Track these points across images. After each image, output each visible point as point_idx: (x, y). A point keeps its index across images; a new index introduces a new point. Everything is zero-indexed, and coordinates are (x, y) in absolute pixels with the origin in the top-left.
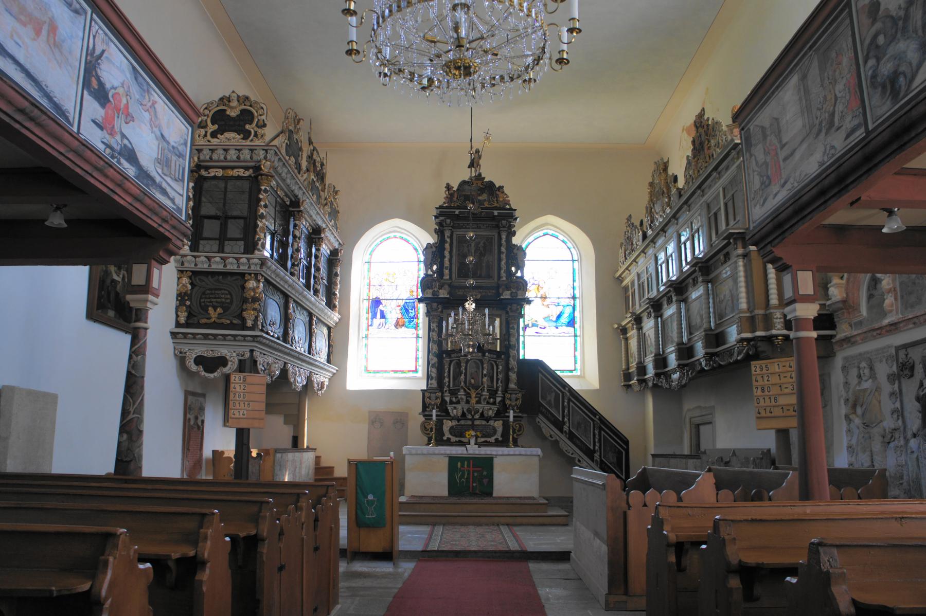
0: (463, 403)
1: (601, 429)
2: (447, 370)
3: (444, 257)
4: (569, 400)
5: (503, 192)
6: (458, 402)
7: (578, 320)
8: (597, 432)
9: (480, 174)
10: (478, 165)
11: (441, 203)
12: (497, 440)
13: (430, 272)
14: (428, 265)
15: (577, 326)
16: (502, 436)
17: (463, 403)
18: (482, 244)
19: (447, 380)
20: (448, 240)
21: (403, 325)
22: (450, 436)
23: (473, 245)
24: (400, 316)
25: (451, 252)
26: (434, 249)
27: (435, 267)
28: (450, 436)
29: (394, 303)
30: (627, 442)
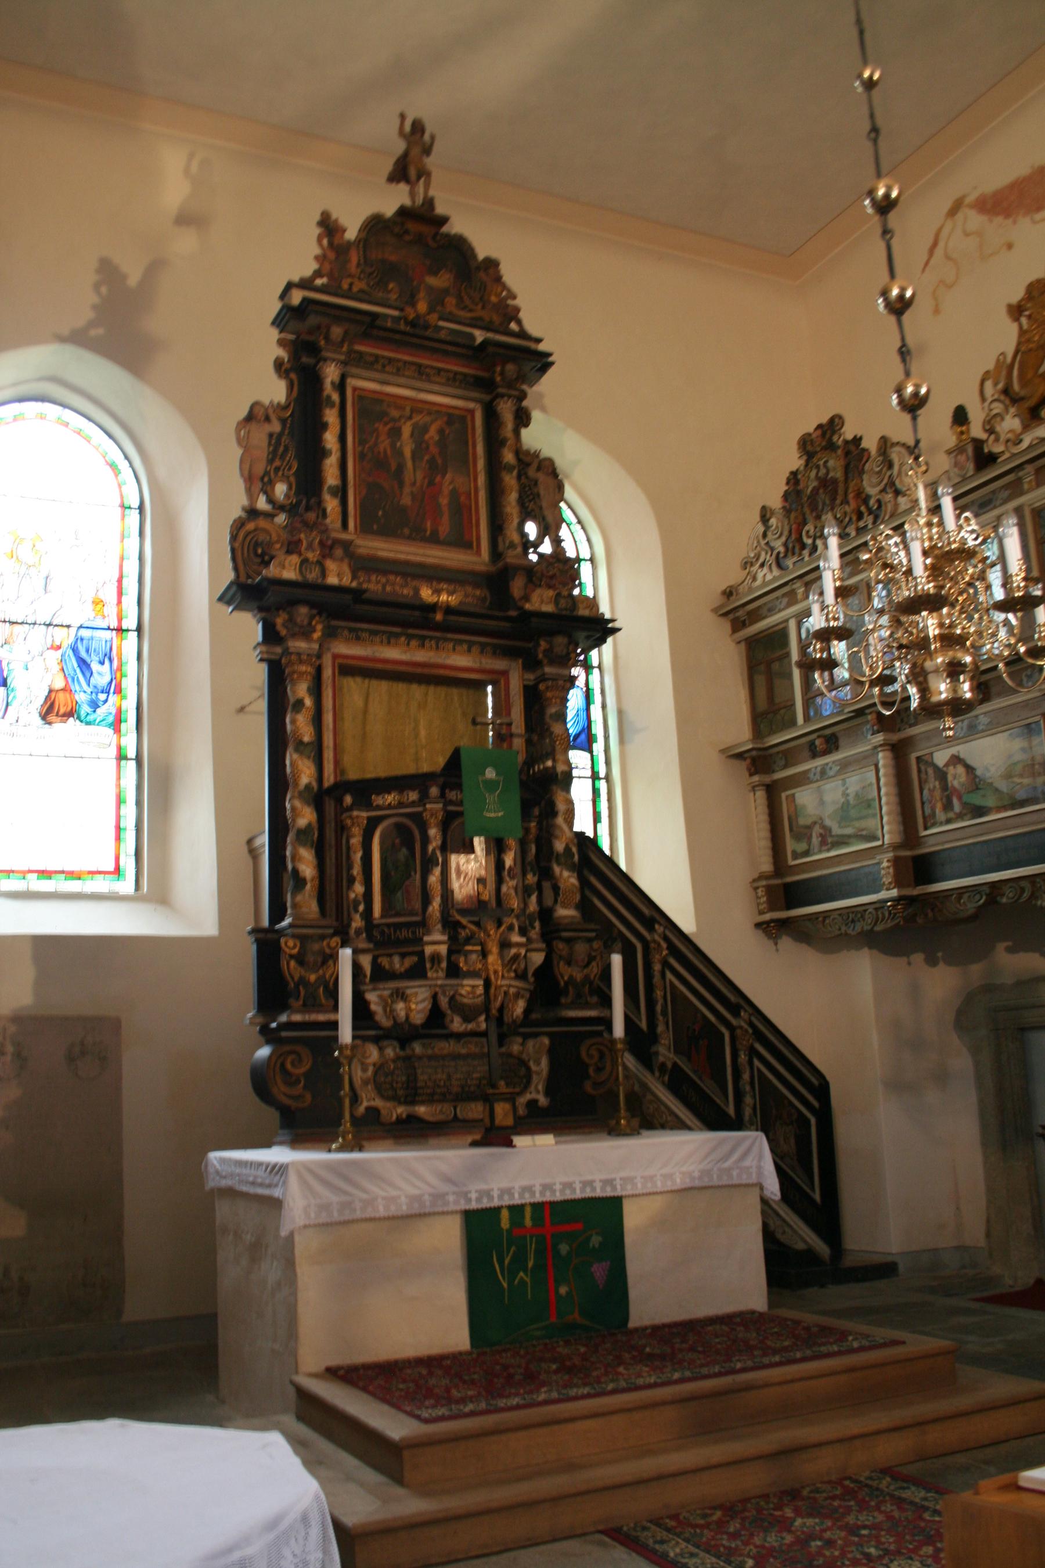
0: (437, 976)
1: (752, 1052)
2: (358, 856)
3: (324, 453)
4: (665, 964)
5: (498, 279)
6: (417, 972)
7: (598, 729)
8: (743, 1057)
9: (429, 203)
10: (424, 173)
11: (308, 273)
12: (532, 1104)
13: (262, 503)
14: (258, 481)
15: (598, 747)
16: (547, 1093)
17: (437, 976)
18: (432, 433)
19: (359, 888)
20: (335, 397)
21: (70, 714)
22: (378, 1103)
23: (407, 430)
24: (59, 684)
25: (342, 438)
26: (276, 427)
27: (280, 489)
28: (378, 1103)
29: (39, 637)
30: (822, 1089)
